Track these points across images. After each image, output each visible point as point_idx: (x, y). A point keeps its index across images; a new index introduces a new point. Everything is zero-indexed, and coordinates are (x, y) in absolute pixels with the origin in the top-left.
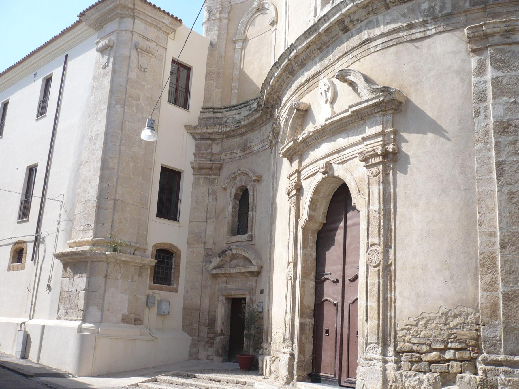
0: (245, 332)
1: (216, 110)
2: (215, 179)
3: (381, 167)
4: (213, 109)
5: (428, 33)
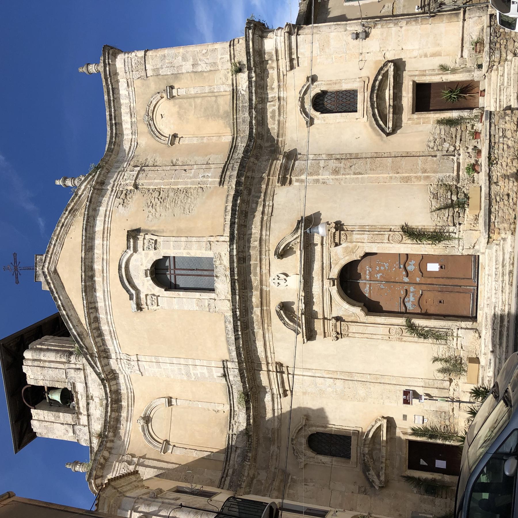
1: (225, 476)
2: (292, 478)
3: (342, 232)
4: (222, 477)
5: (271, 204)
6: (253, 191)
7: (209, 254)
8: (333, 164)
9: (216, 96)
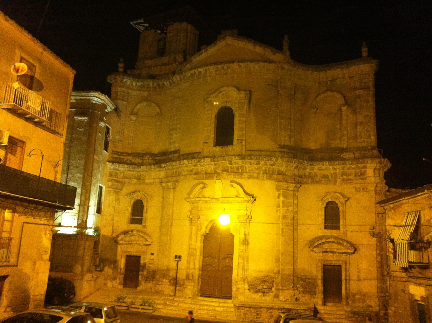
0: (140, 273)
6: (273, 167)
7: (235, 142)
8: (290, 215)
9: (340, 138)
